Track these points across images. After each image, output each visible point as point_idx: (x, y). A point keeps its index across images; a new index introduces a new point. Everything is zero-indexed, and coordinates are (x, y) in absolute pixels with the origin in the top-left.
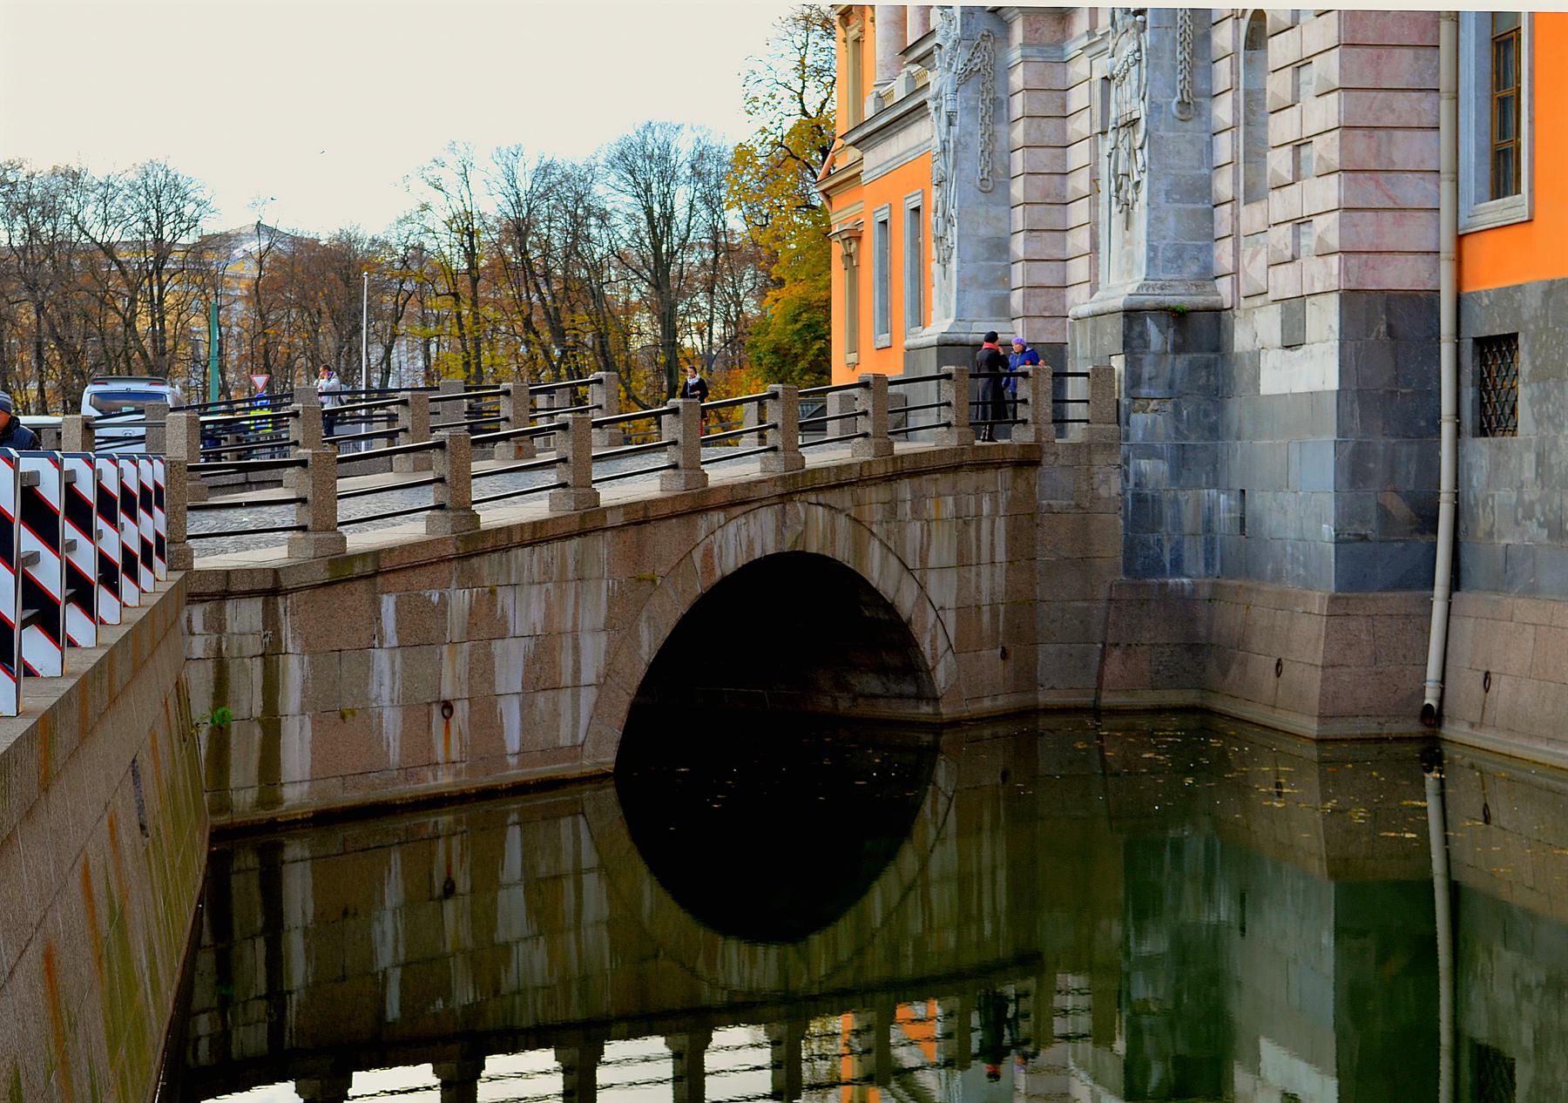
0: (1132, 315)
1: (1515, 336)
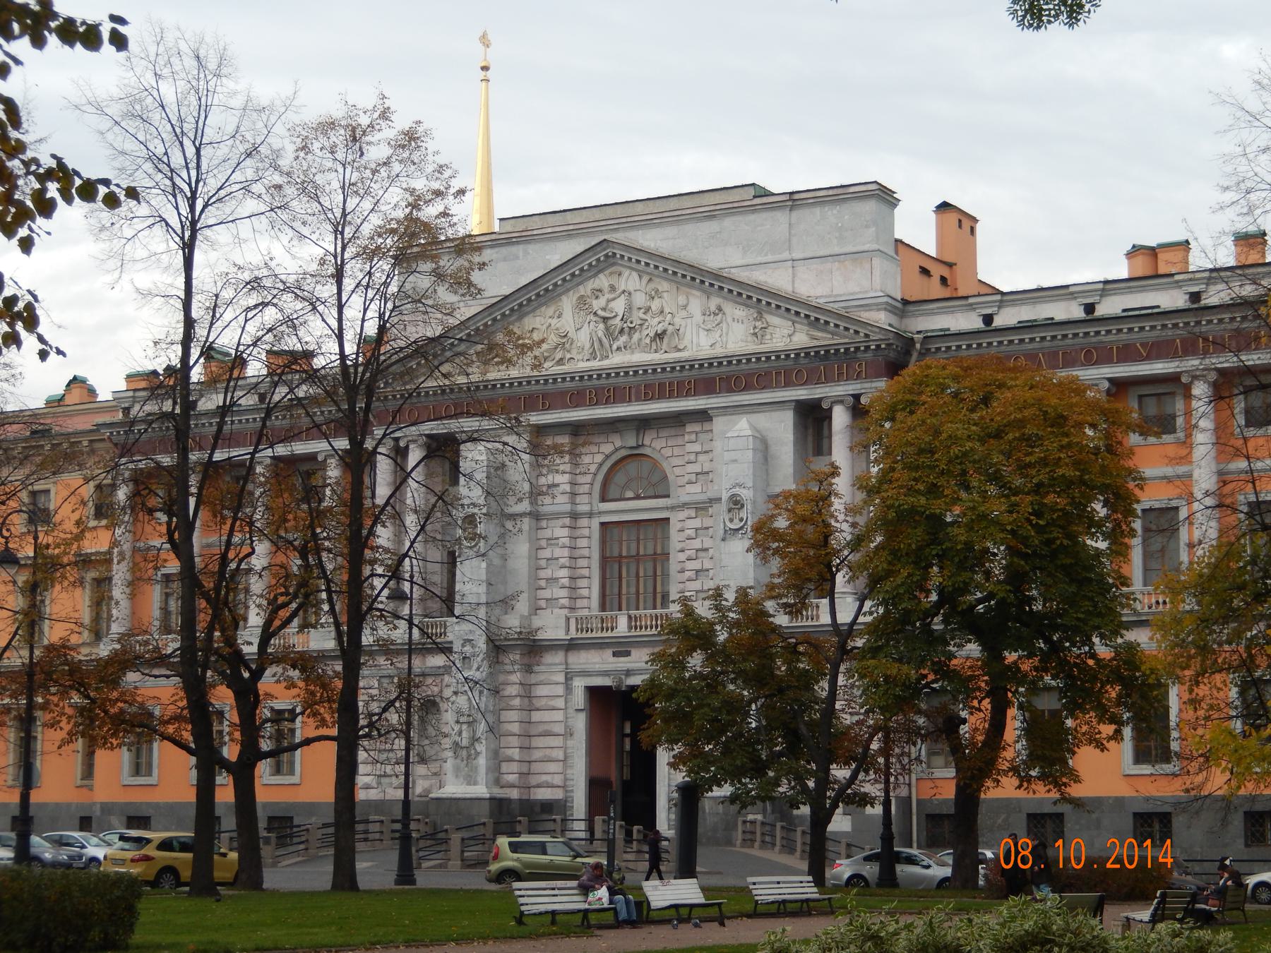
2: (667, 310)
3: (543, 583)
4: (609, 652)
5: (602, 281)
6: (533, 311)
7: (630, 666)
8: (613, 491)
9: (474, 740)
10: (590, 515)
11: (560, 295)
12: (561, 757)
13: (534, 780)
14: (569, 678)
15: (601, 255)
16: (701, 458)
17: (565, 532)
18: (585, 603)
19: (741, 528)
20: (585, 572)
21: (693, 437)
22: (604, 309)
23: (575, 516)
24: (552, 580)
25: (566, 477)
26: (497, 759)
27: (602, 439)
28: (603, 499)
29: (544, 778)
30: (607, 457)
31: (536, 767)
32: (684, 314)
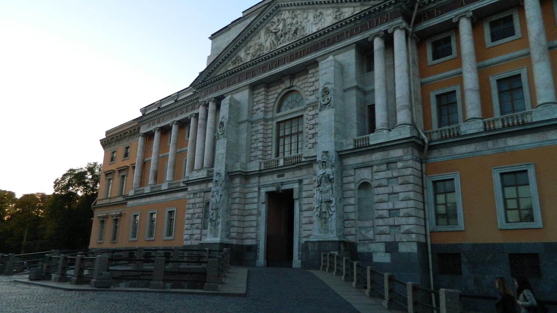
0: (339, 242)
1: (459, 254)
2: (299, 21)
3: (253, 150)
4: (275, 176)
5: (275, 19)
6: (250, 40)
7: (283, 181)
8: (283, 108)
9: (217, 216)
10: (272, 119)
11: (260, 30)
12: (255, 225)
13: (245, 236)
14: (259, 189)
15: (274, 8)
16: (316, 83)
17: (261, 127)
18: (269, 156)
19: (328, 103)
20: (270, 144)
21: (312, 75)
22: (275, 29)
23: (266, 120)
24: (256, 148)
25: (262, 105)
26: (228, 225)
27: (277, 87)
28: (278, 112)
29: (249, 235)
30: (280, 94)
31: (246, 230)
32: (306, 21)
